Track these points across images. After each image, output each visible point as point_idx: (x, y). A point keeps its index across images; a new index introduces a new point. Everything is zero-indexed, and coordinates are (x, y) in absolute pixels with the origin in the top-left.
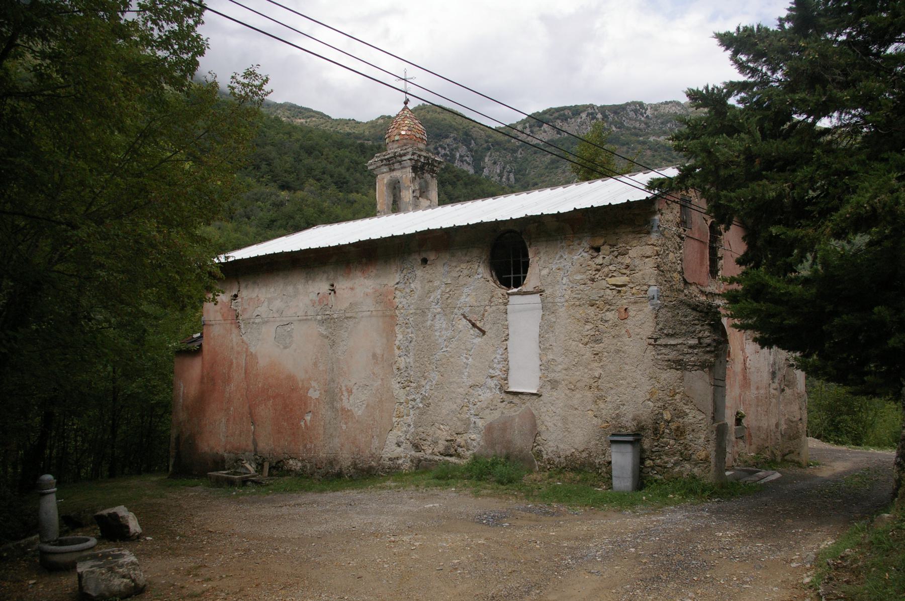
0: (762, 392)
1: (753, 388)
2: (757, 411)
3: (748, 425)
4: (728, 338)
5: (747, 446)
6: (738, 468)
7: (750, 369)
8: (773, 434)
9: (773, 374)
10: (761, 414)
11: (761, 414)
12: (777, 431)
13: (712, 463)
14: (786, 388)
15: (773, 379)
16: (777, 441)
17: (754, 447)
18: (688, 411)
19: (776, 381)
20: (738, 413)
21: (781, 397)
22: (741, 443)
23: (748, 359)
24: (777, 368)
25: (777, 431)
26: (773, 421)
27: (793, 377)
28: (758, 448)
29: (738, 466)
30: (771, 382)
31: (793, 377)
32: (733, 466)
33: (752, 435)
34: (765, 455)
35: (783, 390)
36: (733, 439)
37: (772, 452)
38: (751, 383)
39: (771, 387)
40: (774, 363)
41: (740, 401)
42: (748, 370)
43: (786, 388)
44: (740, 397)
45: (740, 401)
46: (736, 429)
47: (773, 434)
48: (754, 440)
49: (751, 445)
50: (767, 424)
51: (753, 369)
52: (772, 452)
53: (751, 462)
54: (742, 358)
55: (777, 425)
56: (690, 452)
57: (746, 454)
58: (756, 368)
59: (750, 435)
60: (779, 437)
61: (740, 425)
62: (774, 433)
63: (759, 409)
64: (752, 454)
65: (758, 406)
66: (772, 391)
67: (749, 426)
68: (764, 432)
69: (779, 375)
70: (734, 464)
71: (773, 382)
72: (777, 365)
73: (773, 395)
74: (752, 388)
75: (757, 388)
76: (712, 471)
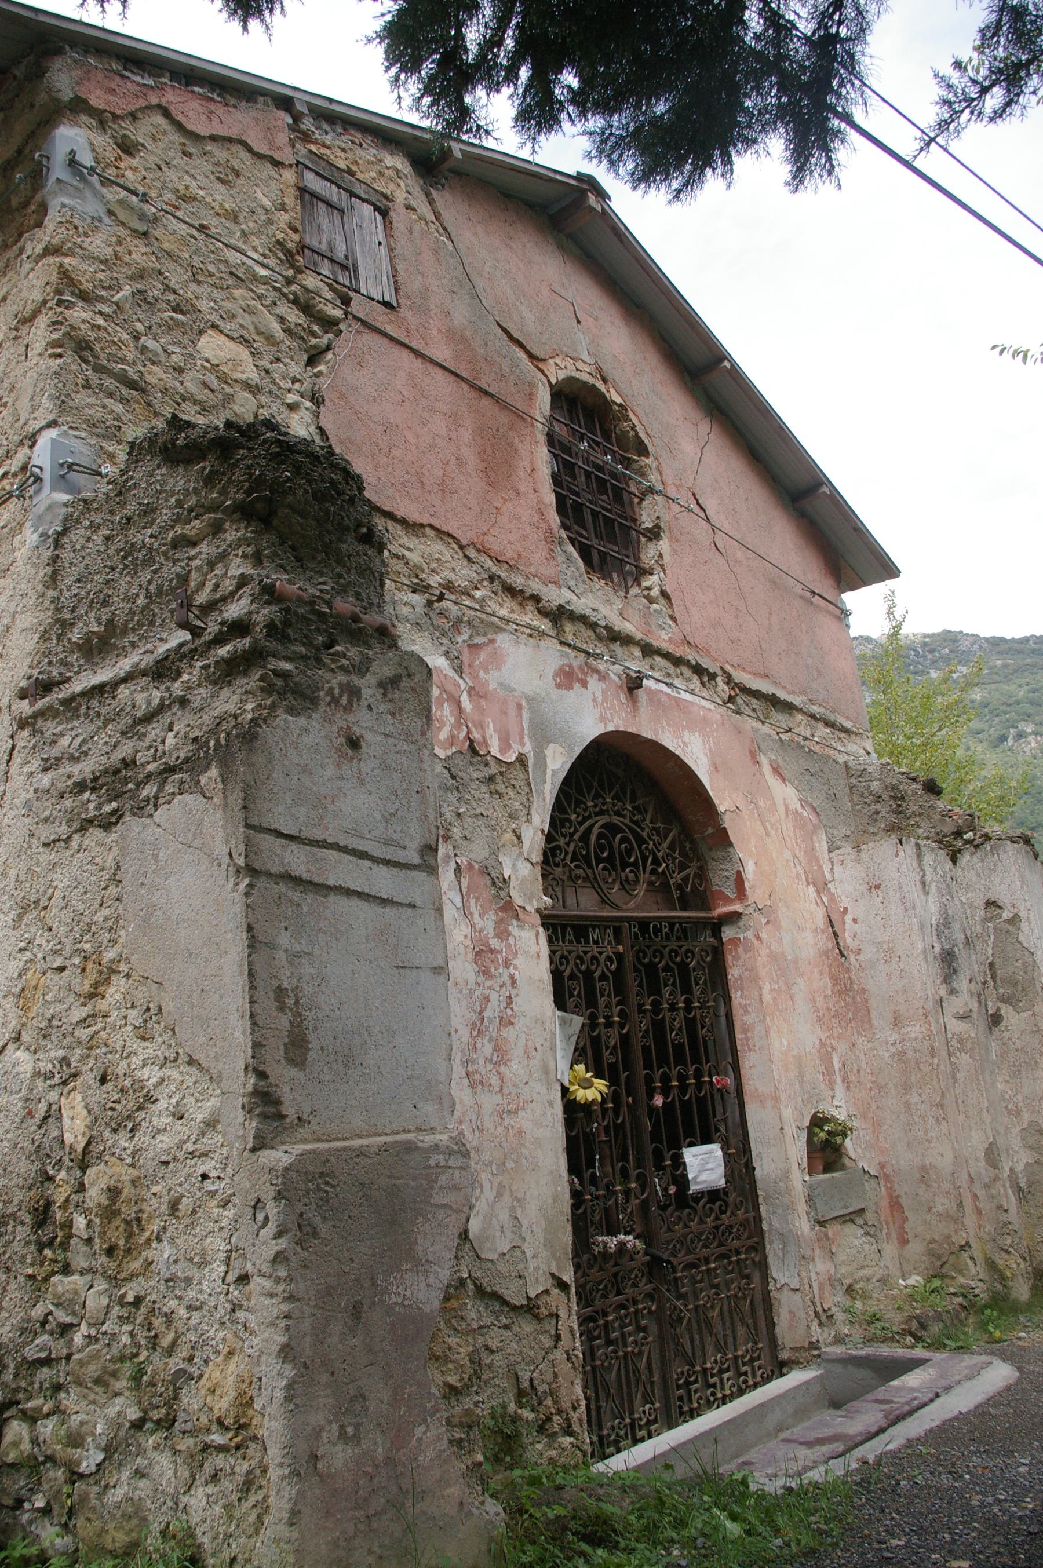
0: (915, 1030)
1: (880, 1020)
2: (908, 1105)
3: (882, 1166)
4: (727, 823)
5: (890, 1250)
6: (838, 1350)
7: (859, 952)
8: (981, 1193)
9: (948, 960)
10: (924, 1118)
11: (924, 1118)
12: (996, 1179)
13: (274, 1453)
14: (1006, 1010)
15: (947, 979)
16: (1004, 1217)
17: (916, 1248)
18: (151, 1075)
19: (962, 983)
20: (818, 1121)
21: (994, 1046)
22: (852, 1238)
23: (848, 918)
24: (960, 937)
25: (996, 1179)
26: (977, 1141)
27: (1025, 964)
28: (931, 1253)
29: (839, 1340)
30: (943, 992)
31: (1025, 964)
32: (813, 1345)
33: (904, 1201)
34: (962, 1280)
35: (996, 1019)
36: (804, 1226)
37: (991, 1265)
38: (873, 1003)
39: (949, 1011)
40: (946, 922)
41: (829, 1071)
42: (852, 958)
43: (1006, 1010)
44: (827, 1060)
45: (829, 1071)
46: (811, 1188)
47: (981, 1193)
48: (914, 1224)
49: (907, 1242)
50: (949, 1157)
51: (869, 953)
52: (991, 1265)
53: (898, 1317)
54: (820, 916)
55: (992, 1155)
56: (175, 1363)
57: (883, 1281)
58: (879, 945)
59: (896, 1204)
60: (1011, 1201)
61: (843, 1167)
62: (987, 1186)
63: (915, 1099)
64: (915, 1280)
65: (907, 1088)
66: (956, 1026)
67: (888, 1170)
68: (946, 1186)
69: (970, 965)
70: (817, 1333)
71: (952, 992)
72: (956, 926)
73: (960, 1041)
74: (875, 1022)
75: (897, 1021)
76: (275, 1526)
